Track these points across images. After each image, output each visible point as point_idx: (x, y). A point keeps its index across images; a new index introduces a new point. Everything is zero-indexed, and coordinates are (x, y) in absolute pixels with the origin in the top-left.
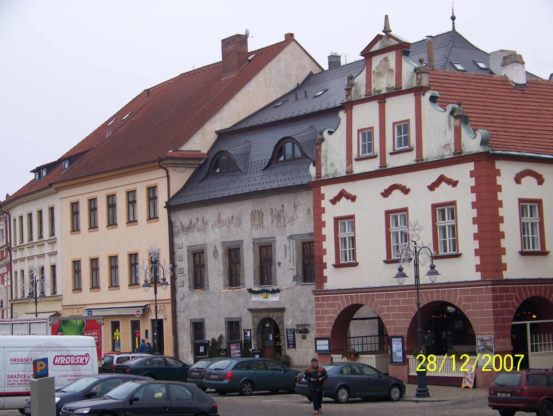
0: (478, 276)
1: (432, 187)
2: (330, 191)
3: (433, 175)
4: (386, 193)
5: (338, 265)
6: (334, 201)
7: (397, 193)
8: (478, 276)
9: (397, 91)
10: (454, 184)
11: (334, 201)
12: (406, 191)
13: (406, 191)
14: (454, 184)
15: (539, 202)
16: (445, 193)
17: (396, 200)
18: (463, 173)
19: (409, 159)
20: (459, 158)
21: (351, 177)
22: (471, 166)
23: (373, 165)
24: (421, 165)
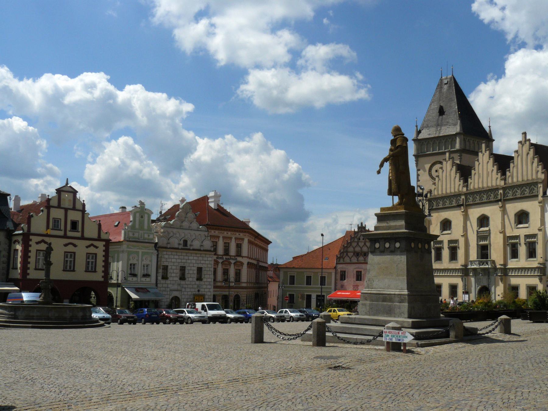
0: (102, 279)
1: (87, 247)
2: (34, 239)
3: (89, 243)
4: (66, 245)
5: (36, 269)
6: (37, 243)
7: (71, 246)
8: (102, 279)
9: (74, 209)
10: (97, 247)
11: (37, 243)
12: (75, 246)
13: (75, 246)
14: (97, 247)
15: (74, 253)
16: (92, 250)
17: (70, 248)
18: (101, 245)
19: (78, 235)
20: (99, 239)
21: (47, 235)
22: (104, 243)
23: (61, 233)
24: (83, 238)
